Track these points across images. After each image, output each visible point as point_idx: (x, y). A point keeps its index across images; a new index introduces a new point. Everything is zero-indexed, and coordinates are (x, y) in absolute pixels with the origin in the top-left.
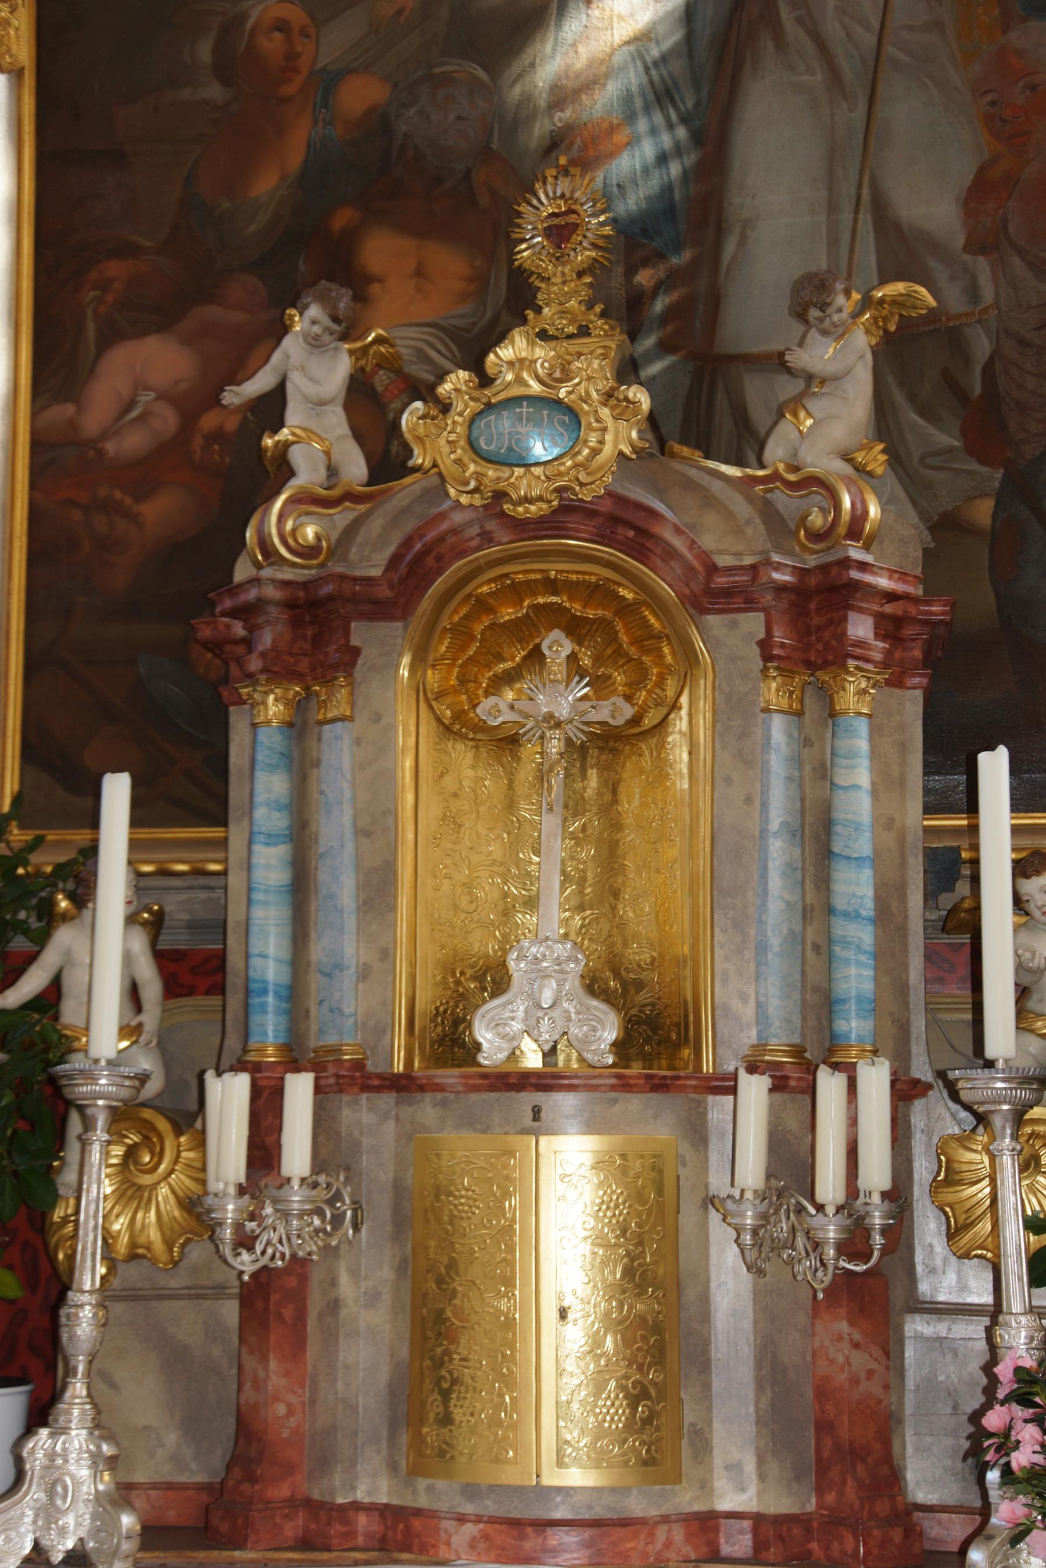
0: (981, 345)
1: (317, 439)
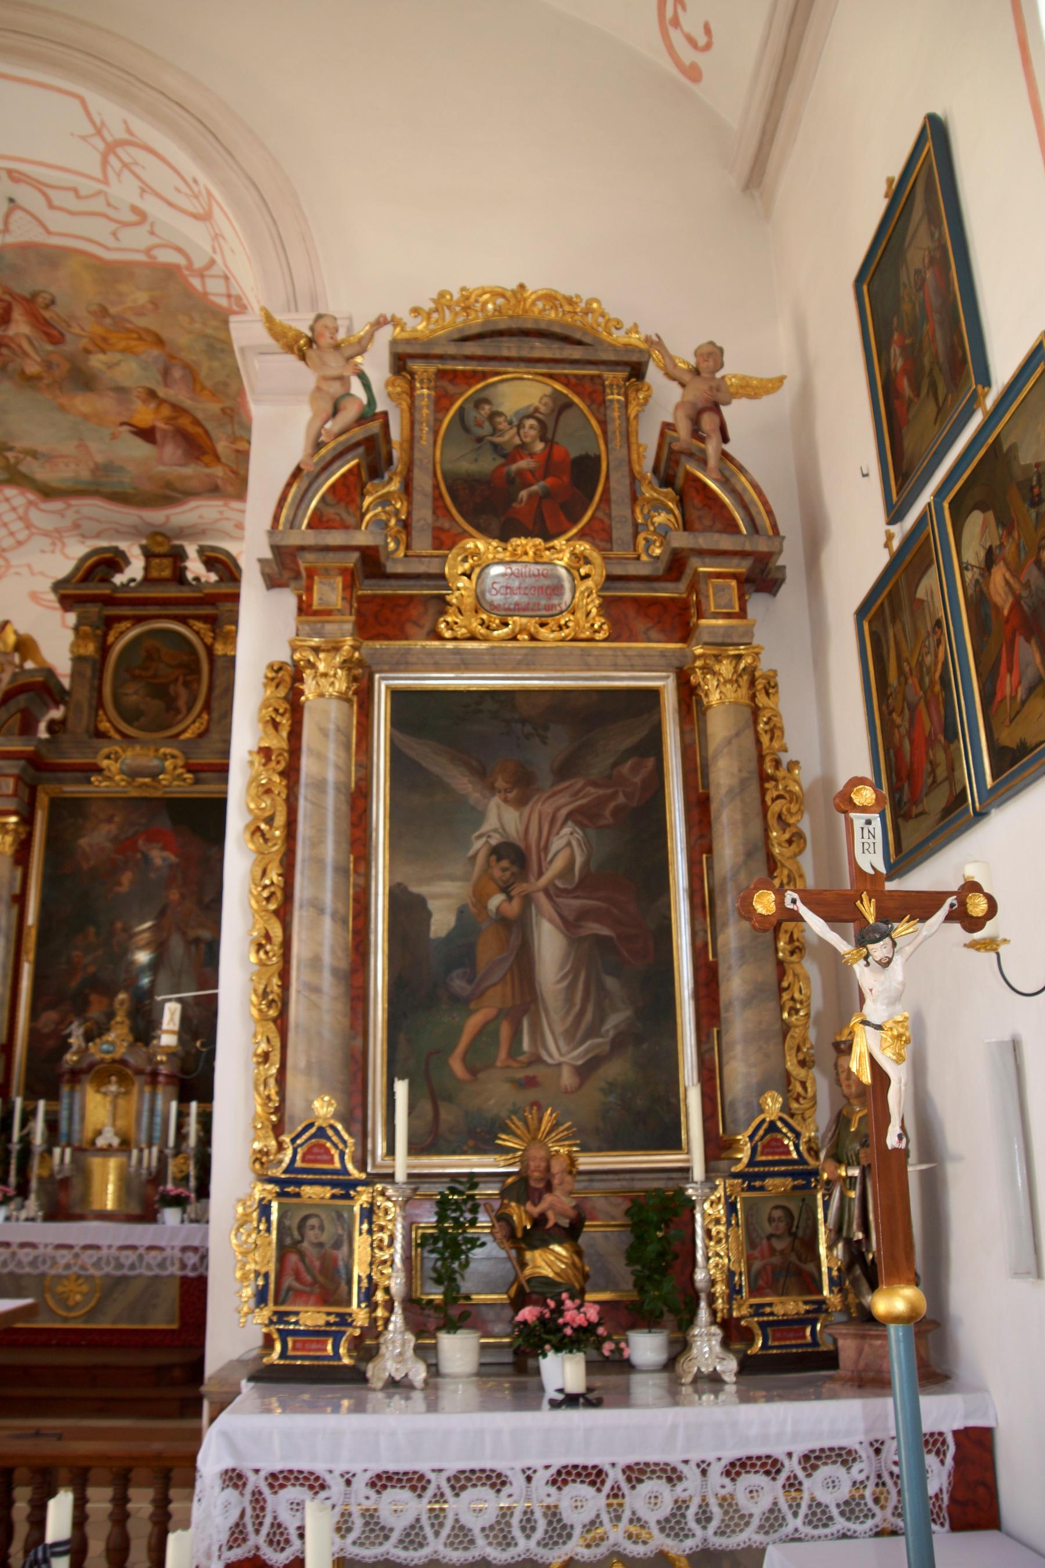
0: (195, 1022)
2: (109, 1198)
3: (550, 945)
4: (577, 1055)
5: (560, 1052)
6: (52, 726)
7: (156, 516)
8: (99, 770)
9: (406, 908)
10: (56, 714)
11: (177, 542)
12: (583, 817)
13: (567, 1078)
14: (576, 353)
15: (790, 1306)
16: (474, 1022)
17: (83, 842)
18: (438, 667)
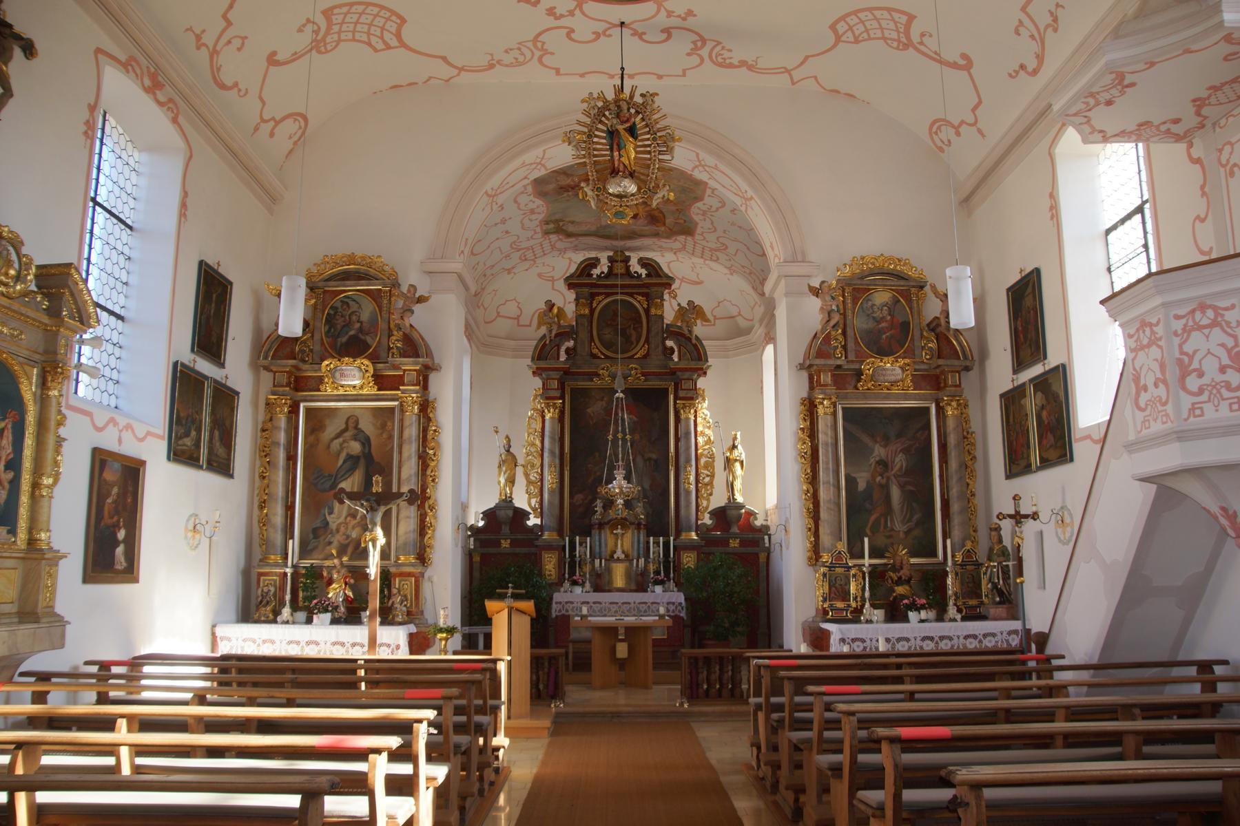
1: (599, 509)
2: (619, 581)
3: (896, 493)
4: (905, 528)
5: (899, 526)
6: (568, 351)
7: (619, 244)
8: (597, 375)
9: (851, 481)
10: (571, 344)
11: (627, 254)
12: (905, 451)
13: (902, 535)
14: (902, 283)
15: (973, 602)
16: (873, 518)
17: (589, 410)
18: (857, 399)
